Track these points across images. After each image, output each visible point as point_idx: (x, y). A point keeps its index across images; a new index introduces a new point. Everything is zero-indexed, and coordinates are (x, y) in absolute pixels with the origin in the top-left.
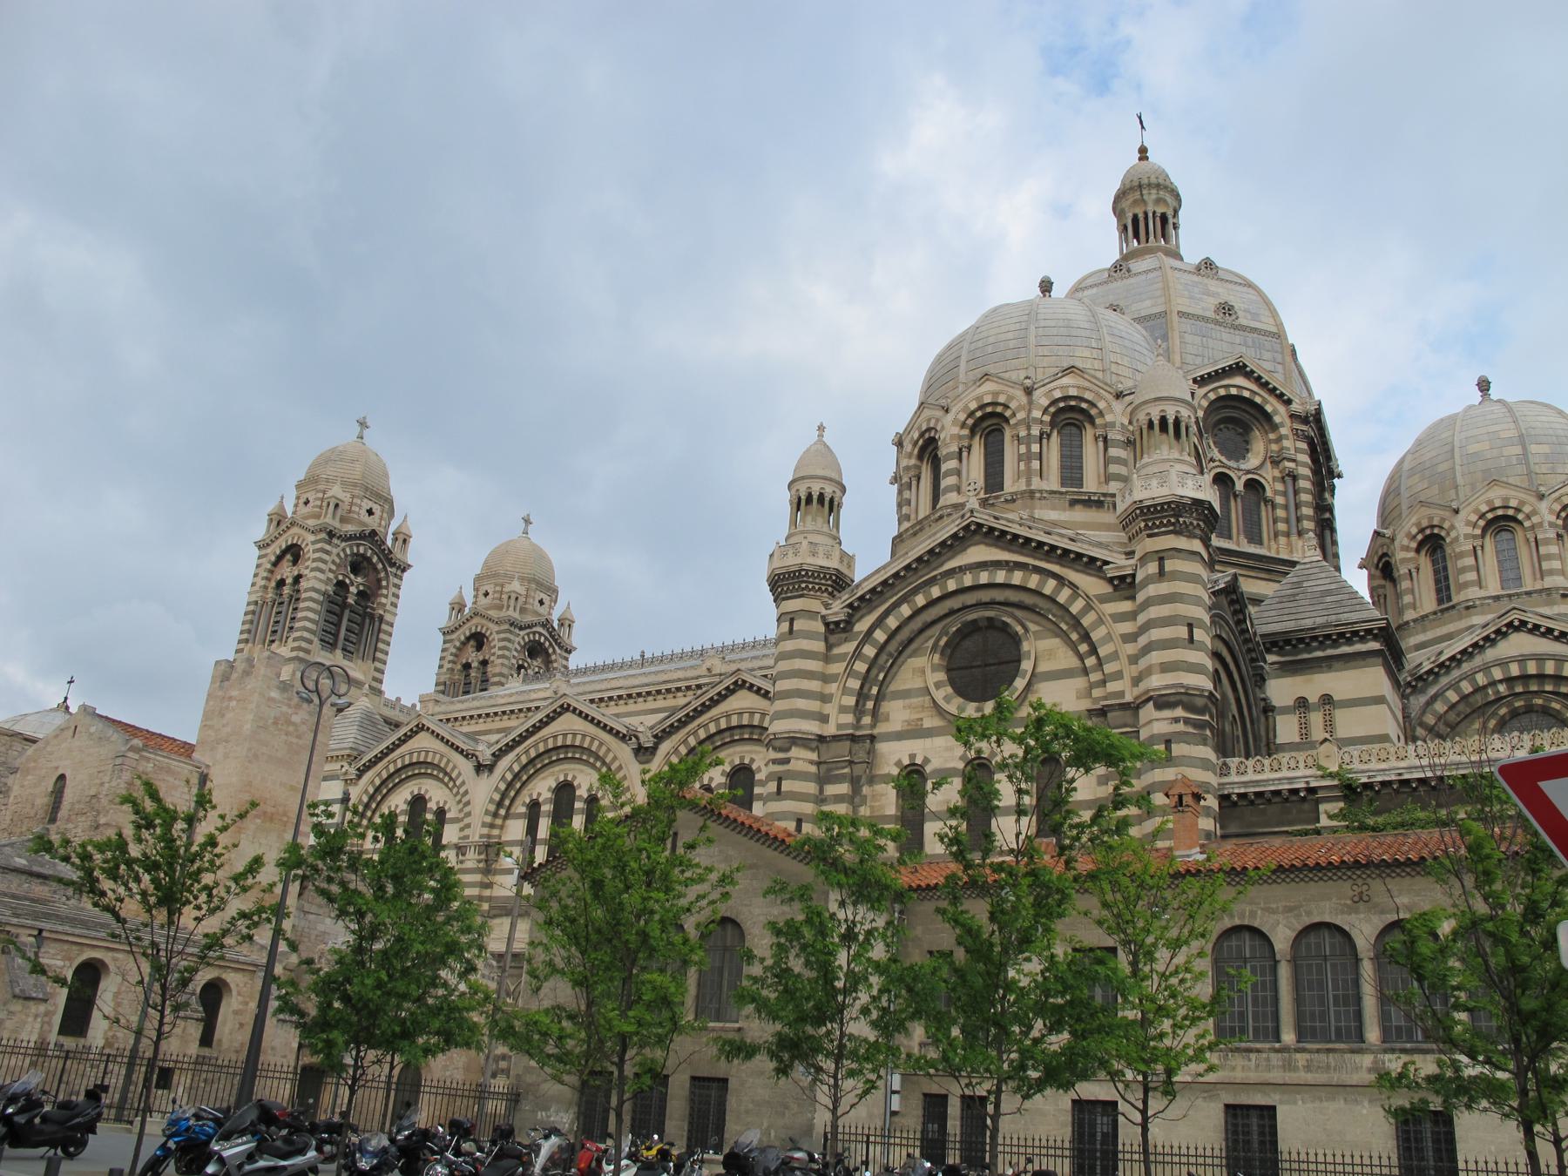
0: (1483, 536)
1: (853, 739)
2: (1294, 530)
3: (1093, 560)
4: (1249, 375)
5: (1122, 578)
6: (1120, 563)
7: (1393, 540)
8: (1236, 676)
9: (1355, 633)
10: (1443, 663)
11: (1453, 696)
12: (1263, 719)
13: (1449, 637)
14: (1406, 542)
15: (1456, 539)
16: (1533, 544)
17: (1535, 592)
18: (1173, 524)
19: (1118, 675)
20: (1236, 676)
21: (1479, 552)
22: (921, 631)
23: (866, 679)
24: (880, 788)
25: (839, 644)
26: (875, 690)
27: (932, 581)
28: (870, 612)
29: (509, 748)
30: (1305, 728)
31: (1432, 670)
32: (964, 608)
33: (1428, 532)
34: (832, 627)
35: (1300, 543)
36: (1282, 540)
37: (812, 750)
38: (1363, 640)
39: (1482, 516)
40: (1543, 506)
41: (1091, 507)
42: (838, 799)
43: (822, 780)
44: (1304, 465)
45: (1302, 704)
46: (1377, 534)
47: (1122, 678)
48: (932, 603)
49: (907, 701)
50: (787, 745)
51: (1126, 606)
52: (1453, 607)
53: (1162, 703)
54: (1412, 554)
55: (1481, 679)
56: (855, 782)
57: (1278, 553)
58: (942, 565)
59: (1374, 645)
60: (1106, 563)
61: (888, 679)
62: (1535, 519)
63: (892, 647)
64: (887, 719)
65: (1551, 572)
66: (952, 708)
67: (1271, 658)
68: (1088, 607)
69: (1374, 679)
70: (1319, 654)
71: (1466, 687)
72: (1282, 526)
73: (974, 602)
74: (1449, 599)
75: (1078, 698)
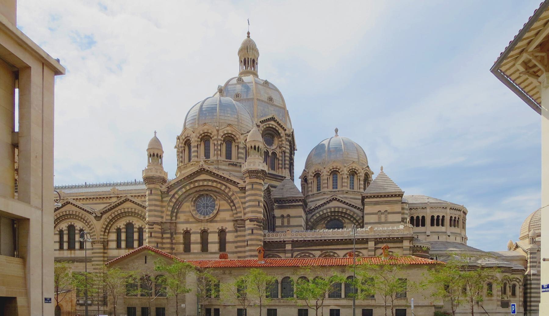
0: (330, 175)
1: (170, 223)
2: (283, 167)
3: (235, 182)
4: (275, 121)
5: (242, 188)
6: (242, 184)
7: (308, 173)
8: (267, 210)
9: (297, 200)
10: (317, 207)
11: (318, 215)
12: (273, 219)
13: (319, 200)
14: (311, 174)
15: (323, 175)
16: (341, 178)
17: (340, 191)
18: (256, 176)
19: (241, 212)
20: (267, 210)
21: (329, 179)
22: (188, 196)
23: (173, 208)
24: (178, 236)
26: (176, 211)
30: (283, 222)
31: (314, 208)
33: (317, 172)
35: (285, 171)
36: (280, 170)
37: (160, 225)
38: (298, 202)
39: (330, 170)
40: (345, 169)
41: (234, 166)
42: (167, 238)
43: (163, 233)
44: (288, 149)
45: (282, 216)
46: (304, 170)
47: (241, 213)
49: (185, 214)
50: (152, 224)
51: (243, 195)
52: (321, 193)
53: (251, 220)
54: (312, 178)
55: (325, 211)
56: (172, 234)
57: (279, 173)
59: (301, 203)
61: (179, 208)
62: (343, 172)
64: (179, 218)
65: (345, 186)
66: (198, 216)
67: (276, 204)
68: (233, 194)
69: (300, 212)
70: (288, 204)
71: (321, 213)
72: (280, 166)
74: (320, 190)
75: (230, 217)
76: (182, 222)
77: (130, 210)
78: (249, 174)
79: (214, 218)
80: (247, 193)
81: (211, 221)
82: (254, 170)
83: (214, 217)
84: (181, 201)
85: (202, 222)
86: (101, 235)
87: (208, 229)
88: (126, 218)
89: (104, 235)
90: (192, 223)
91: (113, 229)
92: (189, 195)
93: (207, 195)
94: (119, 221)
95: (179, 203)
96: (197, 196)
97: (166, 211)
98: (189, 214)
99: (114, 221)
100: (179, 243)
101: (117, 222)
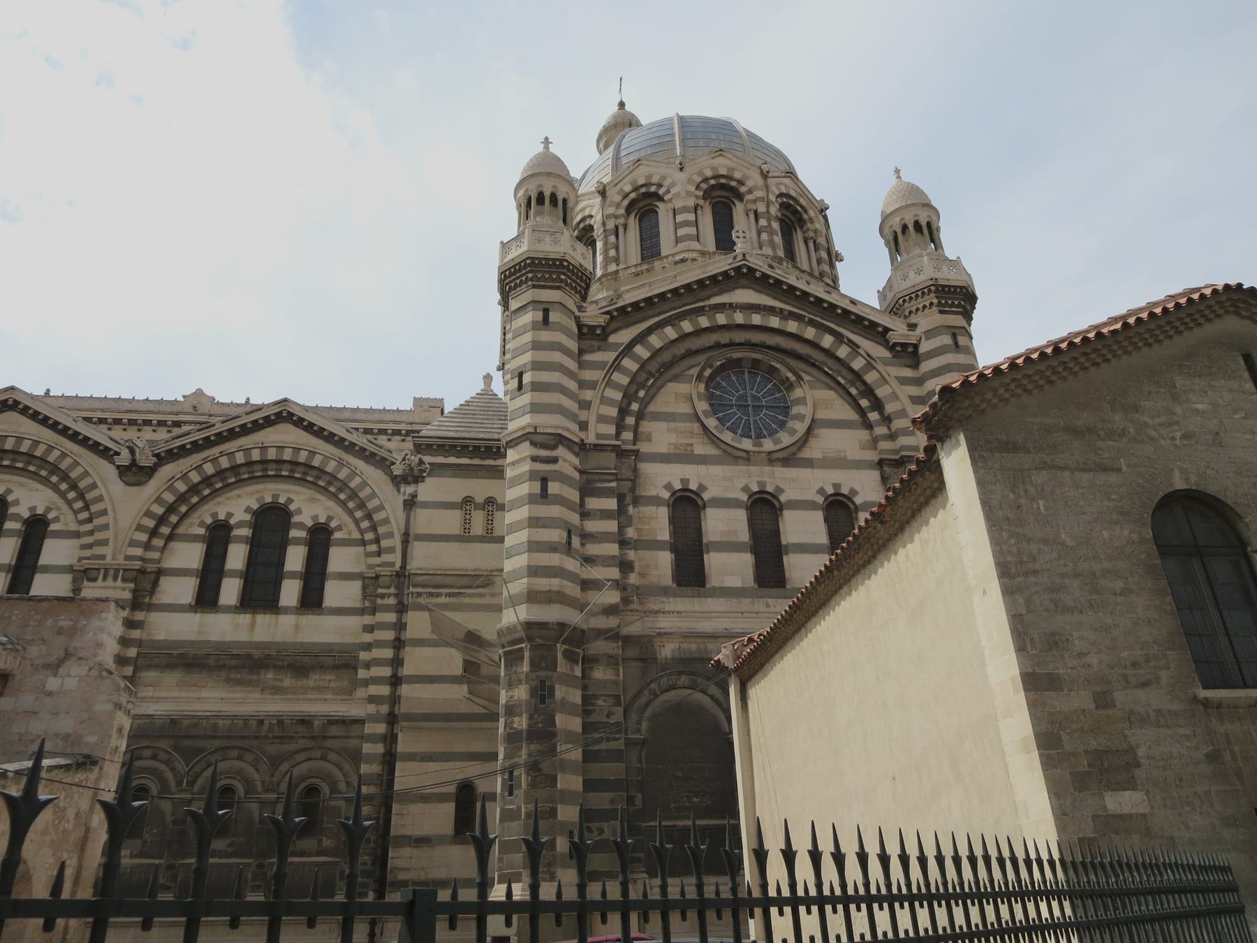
5: (904, 346)
22: (683, 357)
23: (629, 396)
24: (647, 510)
25: (592, 351)
27: (700, 311)
32: (732, 344)
34: (585, 330)
37: (577, 455)
42: (605, 514)
43: (587, 490)
48: (699, 332)
49: (672, 425)
51: (908, 373)
58: (708, 298)
60: (887, 330)
63: (653, 367)
68: (870, 366)
73: (742, 341)
75: (861, 448)
76: (661, 454)
77: (287, 455)
78: (937, 297)
79: (799, 449)
80: (926, 366)
81: (790, 458)
82: (956, 287)
83: (799, 444)
84: (657, 375)
85: (748, 459)
86: (133, 543)
87: (781, 491)
88: (261, 486)
89: (147, 546)
90: (703, 460)
91: (191, 525)
92: (691, 353)
93: (756, 363)
94: (229, 495)
95: (647, 380)
96: (719, 363)
97: (598, 401)
98: (687, 424)
100: (656, 545)
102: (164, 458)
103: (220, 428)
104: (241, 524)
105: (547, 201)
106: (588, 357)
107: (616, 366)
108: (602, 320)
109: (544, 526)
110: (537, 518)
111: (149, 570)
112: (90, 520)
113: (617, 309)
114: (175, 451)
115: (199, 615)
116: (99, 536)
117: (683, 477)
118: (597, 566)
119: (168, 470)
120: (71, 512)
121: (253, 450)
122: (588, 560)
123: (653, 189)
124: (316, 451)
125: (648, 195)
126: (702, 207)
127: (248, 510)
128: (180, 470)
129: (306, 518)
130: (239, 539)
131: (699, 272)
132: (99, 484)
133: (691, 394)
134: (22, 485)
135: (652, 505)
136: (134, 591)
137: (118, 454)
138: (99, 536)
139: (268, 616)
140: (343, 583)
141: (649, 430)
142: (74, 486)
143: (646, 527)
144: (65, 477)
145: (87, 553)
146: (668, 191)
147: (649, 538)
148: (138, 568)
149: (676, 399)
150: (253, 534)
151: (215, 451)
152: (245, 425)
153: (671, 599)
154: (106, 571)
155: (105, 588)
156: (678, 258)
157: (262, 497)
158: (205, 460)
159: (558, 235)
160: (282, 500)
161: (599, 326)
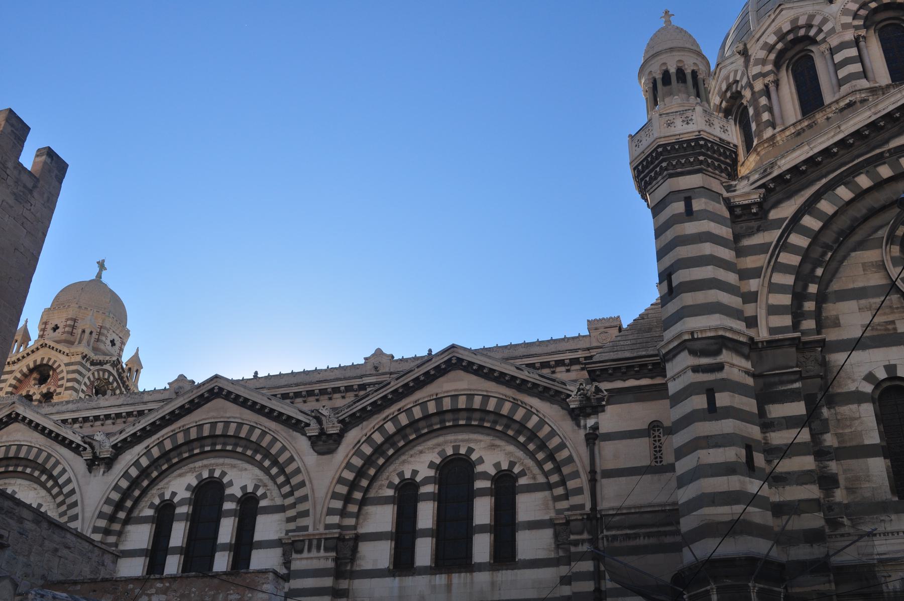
22: (866, 218)
23: (803, 275)
24: (847, 410)
27: (879, 159)
28: (789, 196)
29: (136, 439)
37: (747, 357)
49: (863, 302)
58: (887, 141)
63: (829, 237)
77: (462, 403)
84: (835, 246)
86: (331, 512)
88: (441, 439)
89: (343, 513)
92: (873, 213)
94: (412, 452)
95: (824, 254)
97: (765, 290)
99: (391, 452)
100: (869, 451)
101: (403, 458)
102: (347, 424)
103: (395, 385)
104: (182, 502)
105: (674, 79)
106: (747, 242)
107: (783, 245)
108: (755, 197)
109: (717, 446)
110: (708, 436)
111: (347, 537)
112: (291, 493)
113: (773, 180)
114: (358, 415)
115: (397, 579)
116: (301, 507)
117: (887, 363)
118: (790, 484)
119: (353, 435)
120: (276, 488)
121: (428, 403)
122: (777, 480)
123: (802, 32)
124: (490, 394)
125: (797, 41)
126: (864, 37)
127: (431, 465)
128: (364, 432)
129: (235, 490)
130: (427, 497)
131: (868, 113)
132: (296, 457)
133: (883, 261)
134: (233, 466)
135: (852, 403)
136: (336, 560)
137: (308, 425)
138: (301, 507)
139: (463, 575)
140: (534, 532)
141: (835, 314)
142: (275, 462)
143: (847, 431)
144: (267, 454)
145: (292, 526)
146: (820, 31)
147: (854, 443)
148: (337, 535)
149: (864, 270)
150: (439, 489)
151: (394, 409)
152: (417, 378)
153: (893, 517)
154: (310, 541)
155: (312, 558)
156: (842, 104)
157: (444, 450)
158: (386, 420)
159: (689, 114)
160: (463, 451)
161: (755, 203)
